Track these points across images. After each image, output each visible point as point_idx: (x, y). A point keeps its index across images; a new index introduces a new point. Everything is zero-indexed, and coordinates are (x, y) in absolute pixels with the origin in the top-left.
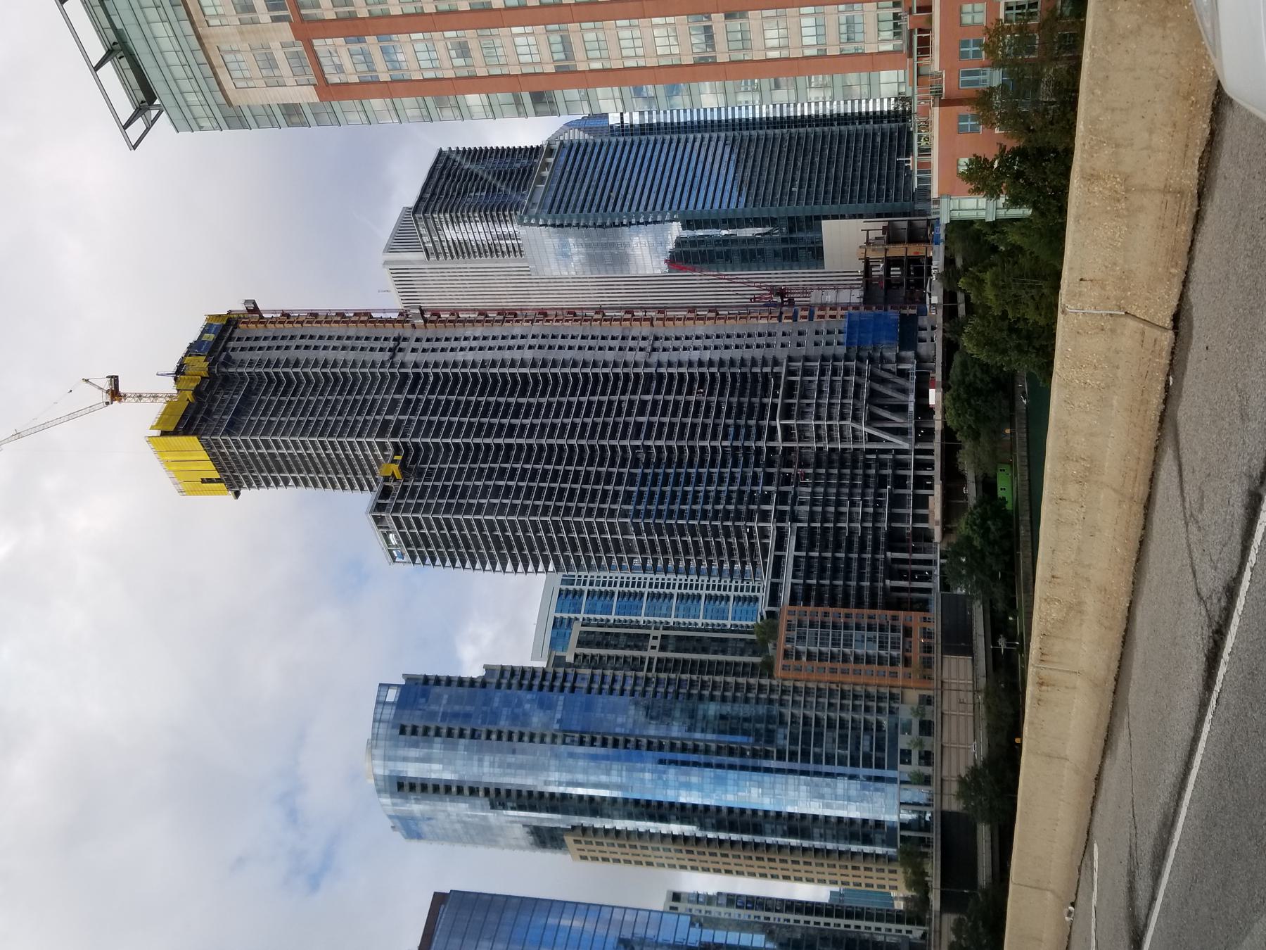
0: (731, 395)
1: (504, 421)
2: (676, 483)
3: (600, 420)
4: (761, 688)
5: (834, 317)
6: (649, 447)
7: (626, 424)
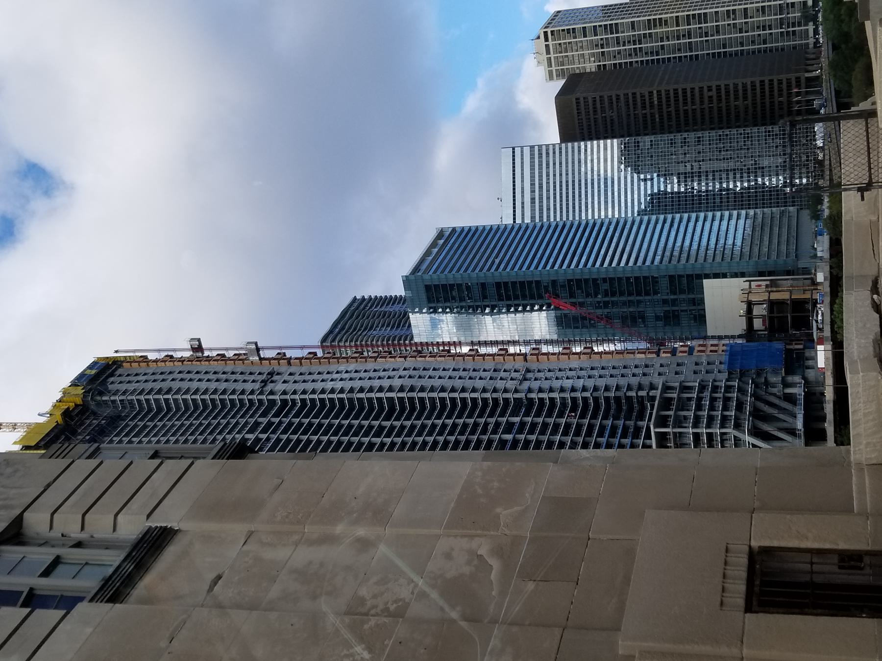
0: (605, 417)
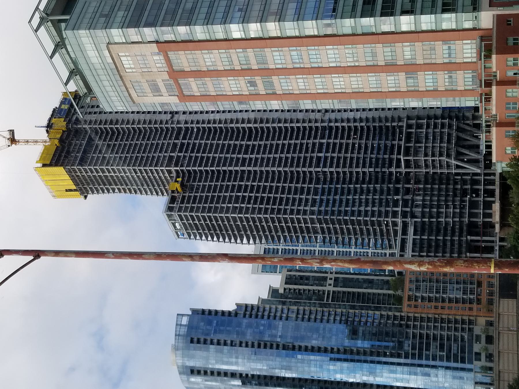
0: (374, 139)
1: (239, 156)
2: (342, 194)
3: (296, 155)
4: (395, 318)
6: (326, 172)
7: (312, 158)
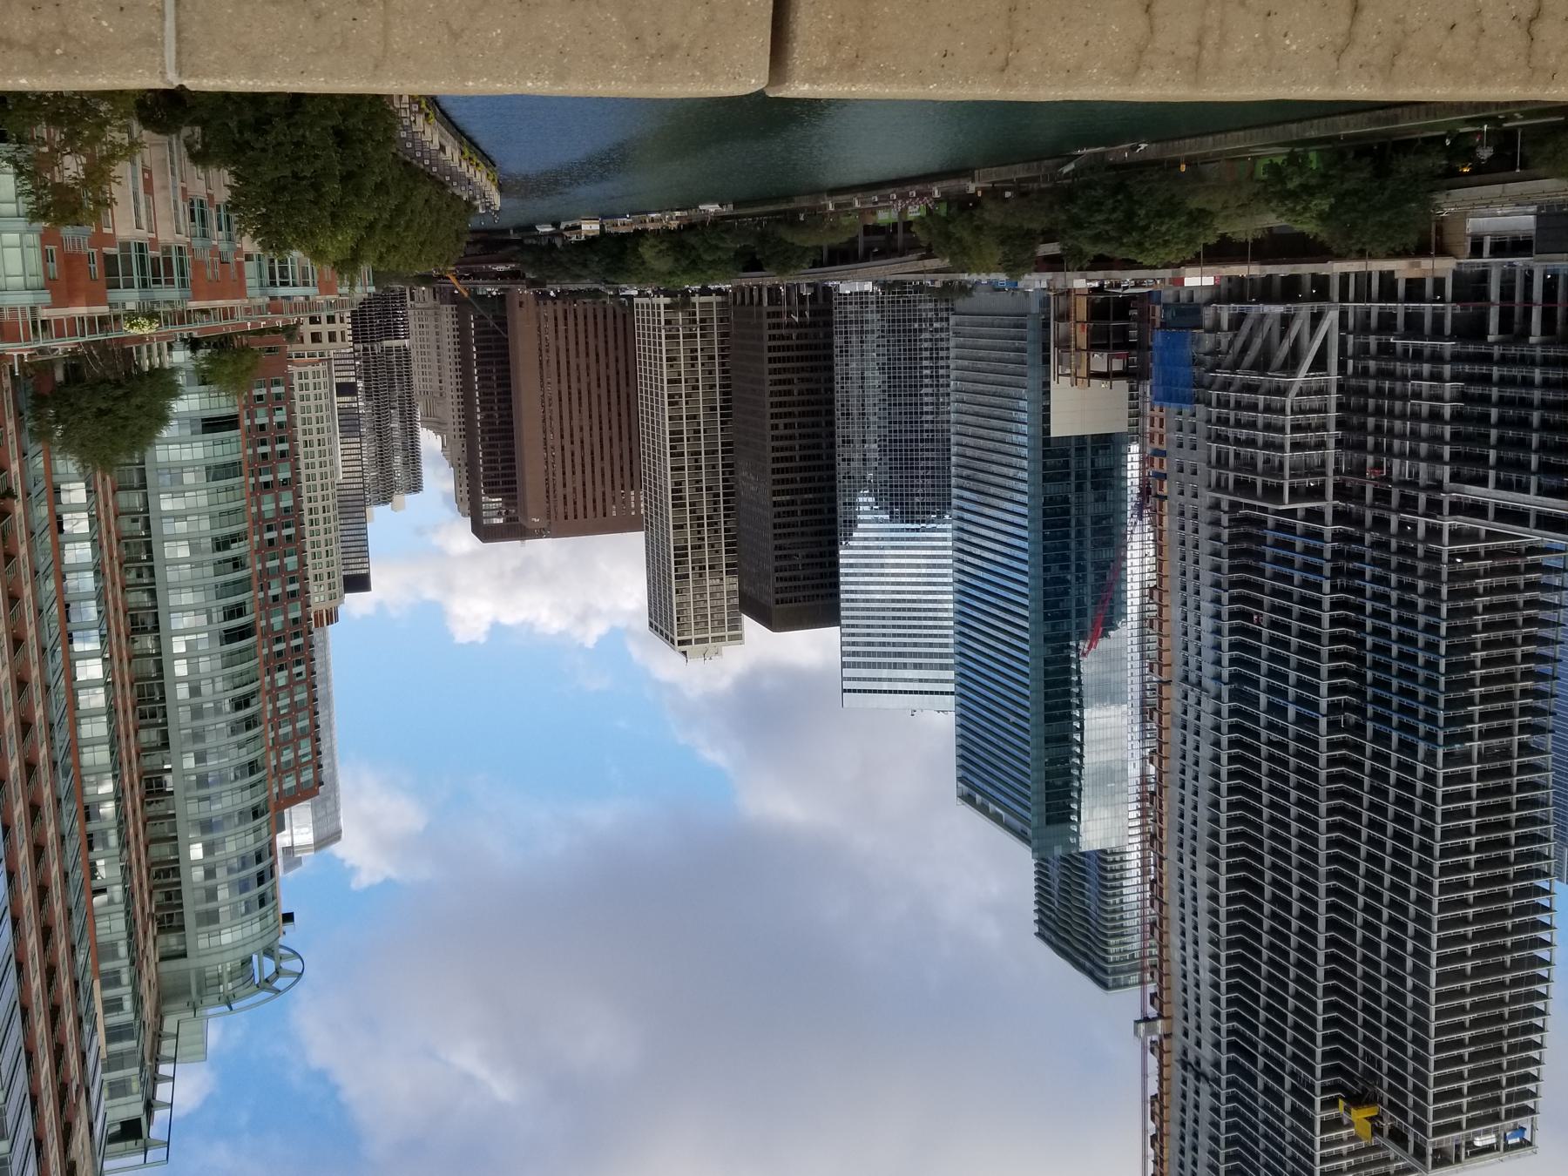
0: (1261, 572)
5: (1161, 420)
